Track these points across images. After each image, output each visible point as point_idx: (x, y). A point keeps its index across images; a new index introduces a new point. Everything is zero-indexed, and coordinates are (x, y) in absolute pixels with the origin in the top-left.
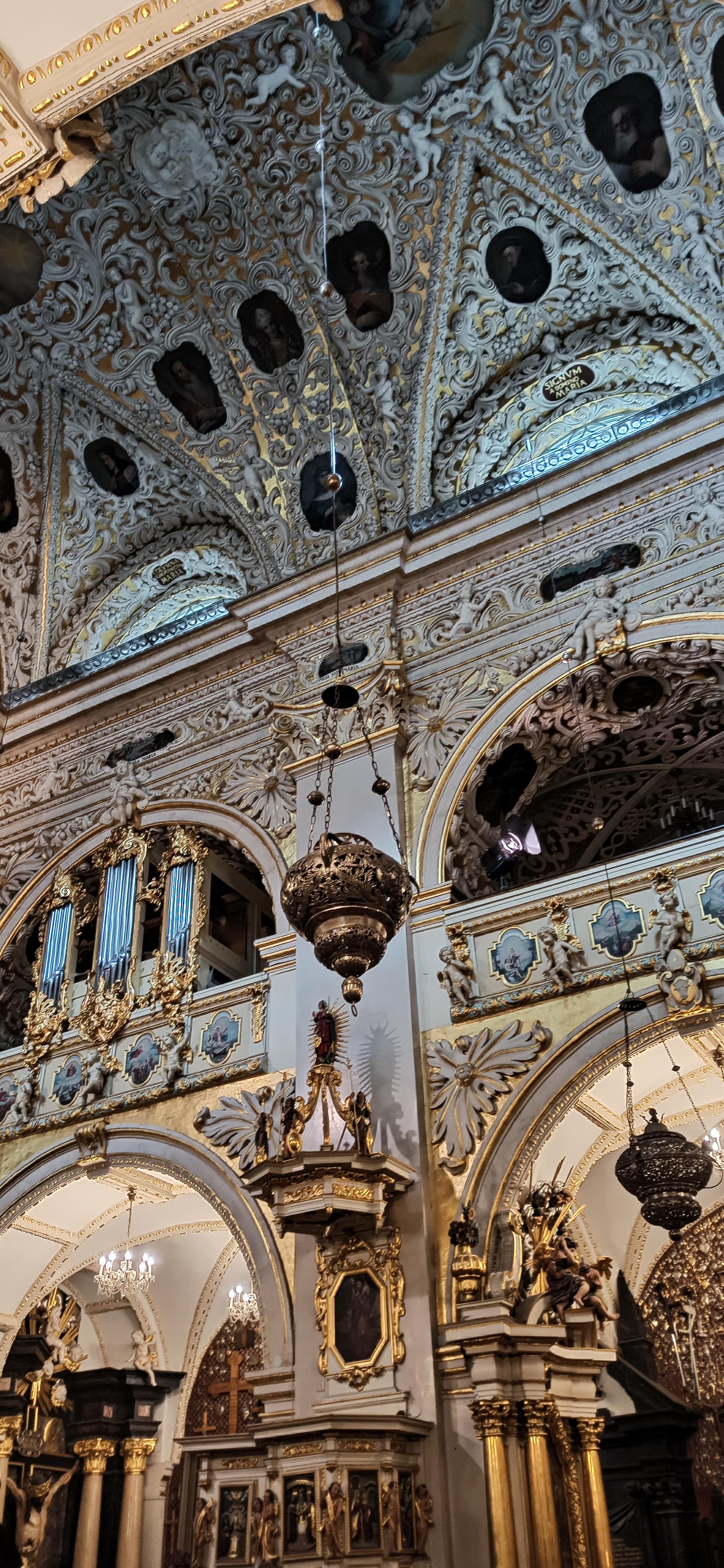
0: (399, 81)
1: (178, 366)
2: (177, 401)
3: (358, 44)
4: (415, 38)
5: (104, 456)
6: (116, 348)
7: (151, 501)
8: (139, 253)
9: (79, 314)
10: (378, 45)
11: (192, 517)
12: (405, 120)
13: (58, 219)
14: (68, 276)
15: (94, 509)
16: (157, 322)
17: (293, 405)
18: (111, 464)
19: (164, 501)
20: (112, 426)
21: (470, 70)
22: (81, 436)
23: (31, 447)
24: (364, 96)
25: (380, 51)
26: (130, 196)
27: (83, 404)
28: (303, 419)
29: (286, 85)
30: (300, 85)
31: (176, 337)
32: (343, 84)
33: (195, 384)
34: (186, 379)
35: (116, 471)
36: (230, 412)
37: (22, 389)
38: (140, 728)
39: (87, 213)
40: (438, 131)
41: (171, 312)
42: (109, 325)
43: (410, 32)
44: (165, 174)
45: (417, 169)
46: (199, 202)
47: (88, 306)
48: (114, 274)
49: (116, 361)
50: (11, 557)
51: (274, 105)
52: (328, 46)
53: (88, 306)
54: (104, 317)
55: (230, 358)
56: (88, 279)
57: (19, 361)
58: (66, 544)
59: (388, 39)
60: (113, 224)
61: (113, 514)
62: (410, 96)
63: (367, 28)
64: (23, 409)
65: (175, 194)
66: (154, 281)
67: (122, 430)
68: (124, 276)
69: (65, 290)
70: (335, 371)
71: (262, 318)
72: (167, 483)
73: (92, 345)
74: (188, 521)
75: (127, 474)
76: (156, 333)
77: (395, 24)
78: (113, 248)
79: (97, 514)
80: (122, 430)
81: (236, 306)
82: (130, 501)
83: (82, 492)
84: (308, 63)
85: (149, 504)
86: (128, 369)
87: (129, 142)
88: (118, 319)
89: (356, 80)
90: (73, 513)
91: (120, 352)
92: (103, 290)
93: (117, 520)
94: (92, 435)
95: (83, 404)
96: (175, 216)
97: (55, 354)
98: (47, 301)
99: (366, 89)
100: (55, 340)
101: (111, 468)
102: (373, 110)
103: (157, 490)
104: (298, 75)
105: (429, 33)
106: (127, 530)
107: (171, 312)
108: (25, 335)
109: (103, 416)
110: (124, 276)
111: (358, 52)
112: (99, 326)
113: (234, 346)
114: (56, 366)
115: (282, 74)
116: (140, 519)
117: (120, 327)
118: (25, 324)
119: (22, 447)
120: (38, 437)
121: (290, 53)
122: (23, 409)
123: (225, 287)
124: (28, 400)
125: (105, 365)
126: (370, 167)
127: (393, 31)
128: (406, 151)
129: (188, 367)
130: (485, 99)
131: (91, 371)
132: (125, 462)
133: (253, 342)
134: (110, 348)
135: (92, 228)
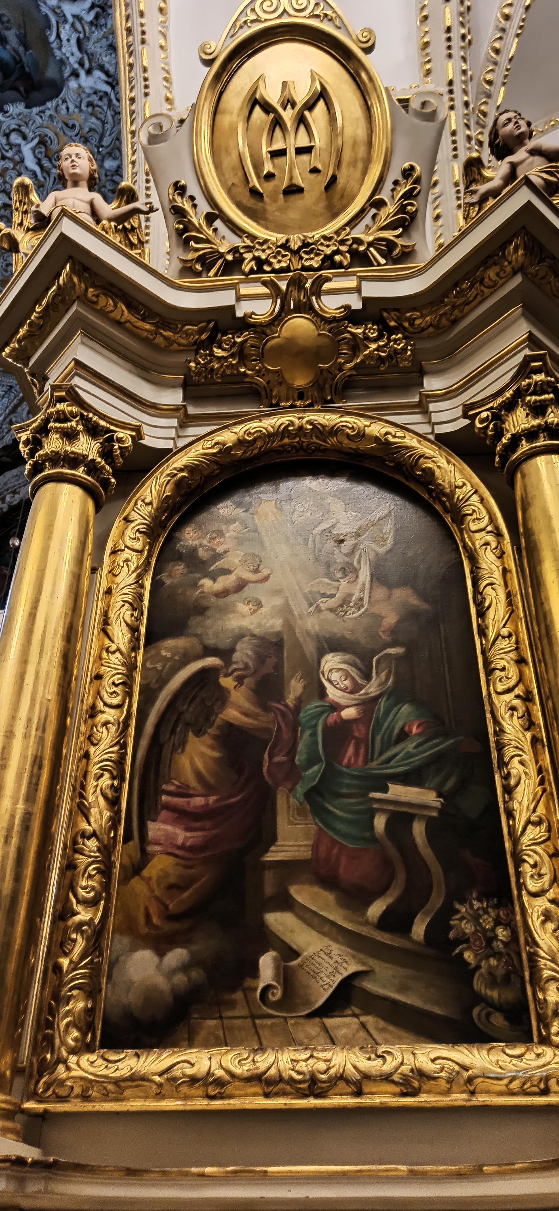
0: (51, 73)
3: (22, 89)
4: (26, 48)
10: (25, 76)
12: (73, 84)
21: (53, 19)
24: (54, 103)
25: (29, 75)
29: (33, 150)
30: (36, 140)
32: (43, 112)
40: (87, 65)
43: (21, 49)
45: (106, 93)
51: (46, 163)
52: (17, 111)
59: (23, 67)
62: (61, 72)
63: (13, 78)
77: (14, 58)
84: (23, 129)
89: (43, 103)
99: (50, 99)
102: (64, 101)
104: (29, 139)
105: (25, 36)
111: (27, 91)
115: (27, 149)
121: (15, 138)
126: (99, 123)
127: (18, 61)
128: (95, 93)
130: (70, 19)
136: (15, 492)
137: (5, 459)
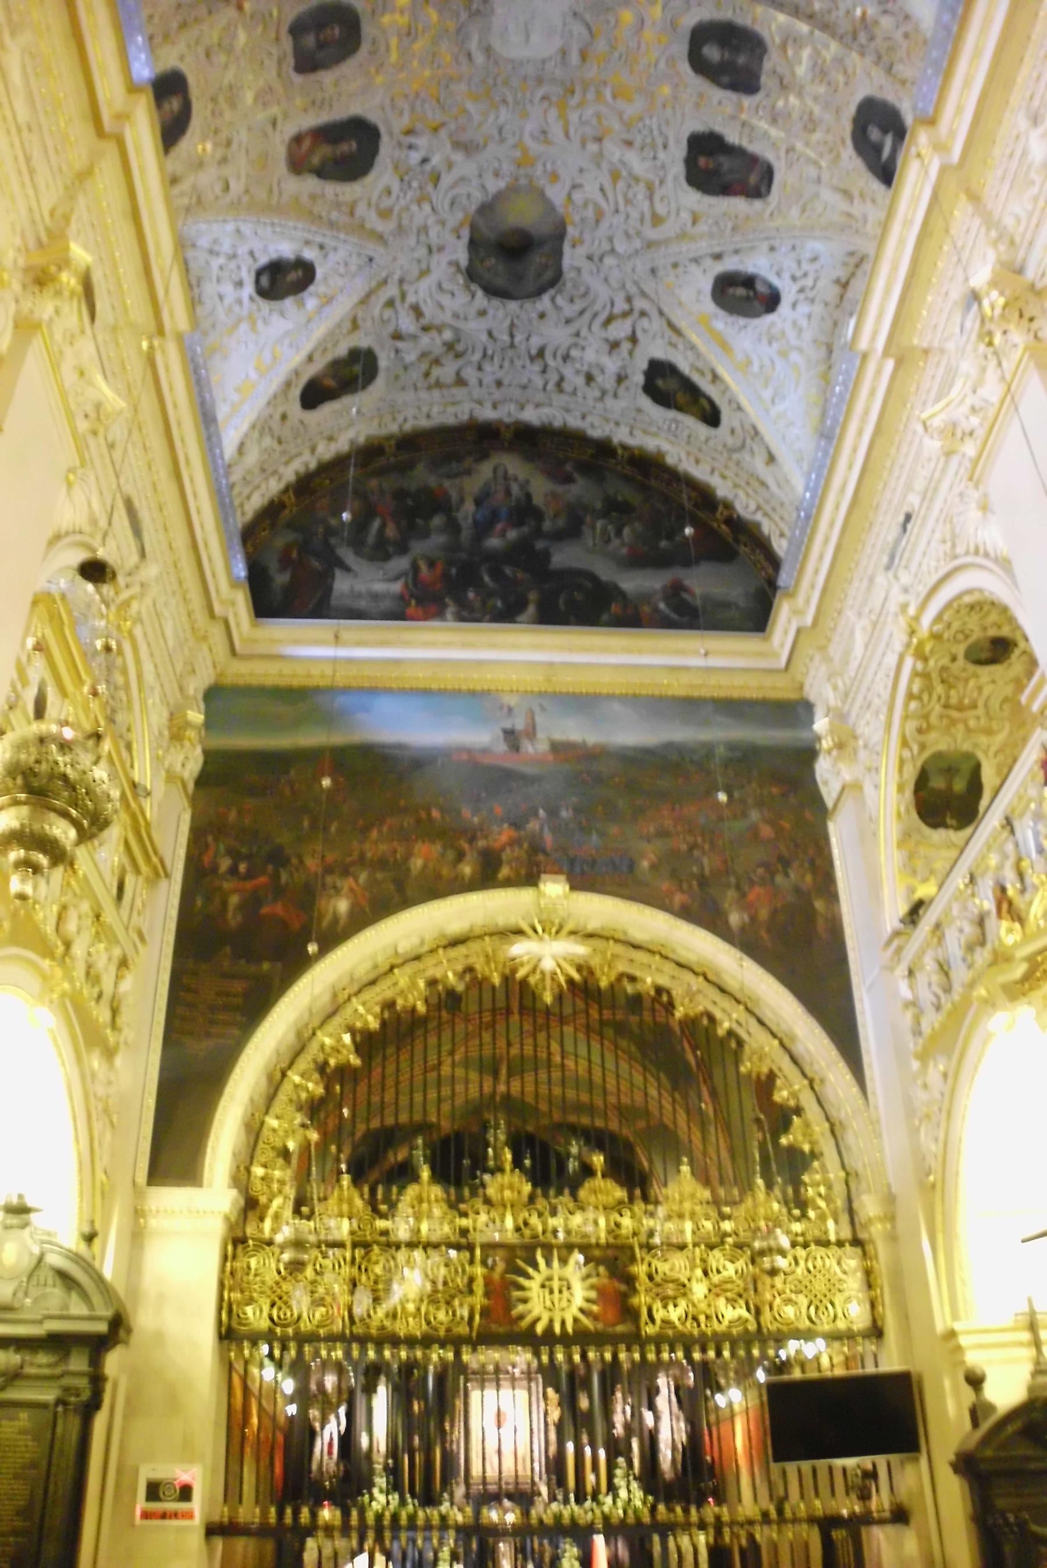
1: (702, 161)
2: (725, 190)
5: (731, 291)
6: (651, 198)
7: (802, 290)
8: (589, 112)
9: (603, 203)
11: (842, 274)
13: (518, 154)
14: (568, 185)
15: (765, 341)
16: (654, 146)
17: (800, 95)
18: (741, 291)
19: (809, 282)
20: (708, 262)
22: (699, 292)
23: (675, 338)
26: (540, 81)
27: (675, 266)
28: (816, 99)
31: (678, 142)
33: (726, 163)
34: (720, 167)
35: (751, 294)
36: (770, 156)
37: (629, 299)
38: (886, 528)
39: (531, 126)
41: (655, 127)
42: (629, 186)
44: (535, 38)
46: (578, 28)
47: (602, 189)
48: (593, 147)
49: (661, 209)
50: (739, 443)
53: (602, 189)
54: (621, 185)
55: (722, 112)
56: (581, 170)
57: (606, 280)
58: (767, 394)
60: (553, 113)
61: (783, 333)
64: (643, 314)
65: (558, 43)
66: (621, 118)
67: (718, 257)
68: (599, 140)
69: (577, 196)
70: (804, 28)
71: (712, 53)
72: (794, 265)
73: (635, 215)
74: (843, 280)
75: (760, 288)
76: (662, 155)
78: (572, 130)
79: (770, 343)
80: (718, 257)
81: (685, 68)
82: (784, 307)
83: (746, 335)
85: (802, 296)
86: (673, 205)
87: (488, 50)
88: (630, 174)
90: (749, 363)
91: (657, 198)
92: (598, 165)
93: (791, 335)
94: (707, 284)
95: (675, 266)
96: (574, 57)
97: (620, 247)
98: (577, 218)
100: (611, 239)
101: (744, 295)
103: (794, 278)
106: (808, 336)
107: (655, 127)
108: (590, 258)
109: (696, 260)
110: (599, 140)
112: (625, 195)
113: (715, 101)
114: (629, 257)
116: (809, 317)
117: (637, 180)
118: (582, 251)
119: (671, 344)
120: (671, 325)
122: (643, 314)
123: (662, 65)
124: (639, 304)
125: (657, 220)
129: (710, 154)
131: (651, 234)
132: (749, 281)
133: (726, 79)
134: (647, 203)
135: (544, 132)
136: (331, 439)
137: (330, 382)
